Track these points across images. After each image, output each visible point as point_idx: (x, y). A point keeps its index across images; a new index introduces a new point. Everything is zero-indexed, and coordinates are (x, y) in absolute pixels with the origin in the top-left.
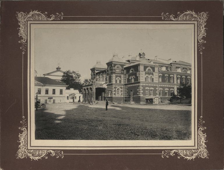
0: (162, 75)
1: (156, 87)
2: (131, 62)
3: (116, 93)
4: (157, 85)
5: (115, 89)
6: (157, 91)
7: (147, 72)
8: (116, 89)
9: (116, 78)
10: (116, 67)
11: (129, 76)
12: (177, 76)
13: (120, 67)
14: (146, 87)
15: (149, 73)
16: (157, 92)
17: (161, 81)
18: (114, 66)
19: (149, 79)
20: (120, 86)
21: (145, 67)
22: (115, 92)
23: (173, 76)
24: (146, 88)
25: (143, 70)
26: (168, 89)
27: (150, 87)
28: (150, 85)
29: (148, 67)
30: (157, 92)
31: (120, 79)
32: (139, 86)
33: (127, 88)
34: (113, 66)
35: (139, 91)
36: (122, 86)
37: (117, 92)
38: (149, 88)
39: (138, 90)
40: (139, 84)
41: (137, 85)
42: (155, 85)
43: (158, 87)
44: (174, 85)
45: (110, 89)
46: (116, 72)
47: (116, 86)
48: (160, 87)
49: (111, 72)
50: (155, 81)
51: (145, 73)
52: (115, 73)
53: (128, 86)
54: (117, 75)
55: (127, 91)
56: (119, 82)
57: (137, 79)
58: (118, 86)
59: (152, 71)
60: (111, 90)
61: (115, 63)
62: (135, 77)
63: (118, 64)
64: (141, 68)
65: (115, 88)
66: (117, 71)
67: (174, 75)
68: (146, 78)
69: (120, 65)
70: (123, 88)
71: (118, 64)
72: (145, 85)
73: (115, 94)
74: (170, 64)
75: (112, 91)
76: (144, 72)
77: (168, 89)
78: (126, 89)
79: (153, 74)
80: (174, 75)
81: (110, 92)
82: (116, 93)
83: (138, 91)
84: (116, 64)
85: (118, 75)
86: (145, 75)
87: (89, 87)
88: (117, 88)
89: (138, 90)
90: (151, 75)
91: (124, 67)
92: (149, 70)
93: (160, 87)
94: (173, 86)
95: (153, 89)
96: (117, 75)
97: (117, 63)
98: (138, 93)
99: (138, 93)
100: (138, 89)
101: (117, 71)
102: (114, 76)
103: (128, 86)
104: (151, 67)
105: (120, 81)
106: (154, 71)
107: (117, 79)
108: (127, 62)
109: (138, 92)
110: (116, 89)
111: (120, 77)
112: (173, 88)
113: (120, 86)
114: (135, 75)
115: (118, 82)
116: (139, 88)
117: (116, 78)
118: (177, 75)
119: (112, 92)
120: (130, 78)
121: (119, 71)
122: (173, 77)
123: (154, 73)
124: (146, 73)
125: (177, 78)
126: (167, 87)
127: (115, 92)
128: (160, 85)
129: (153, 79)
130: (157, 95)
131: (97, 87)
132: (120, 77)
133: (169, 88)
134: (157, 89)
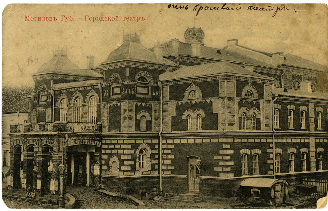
0: (279, 107)
1: (264, 146)
4: (269, 140)
6: (270, 159)
7: (244, 101)
8: (138, 151)
9: (136, 116)
11: (180, 109)
12: (315, 110)
13: (150, 80)
14: (241, 149)
15: (249, 101)
16: (269, 162)
17: (278, 127)
19: (249, 121)
20: (149, 141)
23: (305, 108)
24: (243, 151)
25: (234, 95)
26: (295, 150)
27: (251, 149)
28: (251, 141)
29: (247, 83)
30: (269, 162)
31: (148, 118)
33: (172, 147)
36: (154, 141)
37: (137, 160)
38: (248, 151)
39: (217, 157)
41: (214, 141)
42: (263, 140)
43: (271, 145)
44: (309, 136)
45: (114, 152)
47: (138, 142)
48: (277, 145)
50: (264, 129)
53: (177, 141)
54: (139, 104)
58: (141, 141)
59: (256, 96)
62: (203, 115)
63: (143, 70)
67: (307, 106)
68: (240, 119)
70: (156, 146)
71: (143, 70)
72: (239, 140)
76: (236, 102)
77: (295, 150)
78: (169, 151)
79: (258, 106)
80: (307, 106)
81: (115, 158)
82: (137, 164)
84: (139, 70)
85: (143, 104)
89: (217, 157)
90: (253, 110)
92: (249, 94)
93: (277, 145)
94: (307, 140)
95: (259, 151)
96: (139, 104)
98: (216, 169)
99: (216, 169)
100: (220, 155)
101: (139, 90)
103: (177, 141)
104: (254, 84)
106: (261, 96)
107: (138, 118)
109: (218, 166)
110: (138, 151)
112: (307, 145)
113: (149, 141)
114: (207, 108)
115: (143, 125)
117: (136, 116)
118: (315, 106)
120: (184, 117)
122: (307, 113)
123: (262, 103)
124: (240, 105)
125: (316, 114)
126: (293, 145)
129: (258, 120)
130: (269, 172)
134: (269, 151)
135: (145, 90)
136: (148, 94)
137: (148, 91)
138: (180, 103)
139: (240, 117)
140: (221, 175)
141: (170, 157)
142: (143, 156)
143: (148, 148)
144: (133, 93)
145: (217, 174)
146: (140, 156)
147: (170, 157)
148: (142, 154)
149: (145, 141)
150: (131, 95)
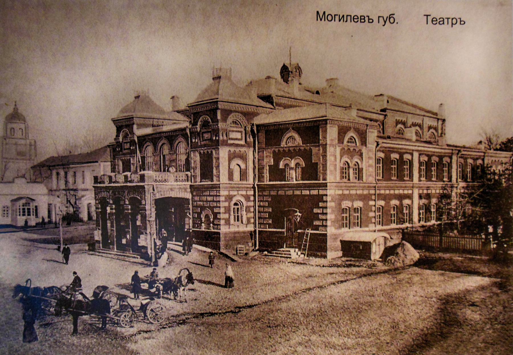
0: (382, 155)
2: (277, 104)
3: (232, 217)
5: (226, 204)
7: (346, 148)
10: (231, 119)
15: (352, 149)
18: (225, 120)
21: (342, 132)
22: (226, 216)
23: (408, 157)
29: (348, 129)
32: (320, 198)
34: (219, 117)
35: (321, 217)
37: (232, 213)
39: (315, 211)
40: (321, 192)
41: (314, 192)
42: (366, 192)
43: (373, 197)
46: (230, 142)
47: (232, 193)
49: (211, 140)
51: (341, 150)
52: (225, 143)
53: (273, 193)
55: (270, 210)
56: (237, 175)
57: (312, 171)
58: (235, 193)
60: (212, 208)
61: (227, 106)
64: (332, 133)
65: (229, 198)
66: (233, 135)
69: (242, 113)
73: (227, 222)
74: (382, 111)
75: (216, 210)
76: (338, 150)
80: (412, 155)
82: (232, 217)
83: (318, 214)
86: (341, 157)
87: (238, 252)
88: (234, 201)
89: (315, 211)
90: (356, 159)
91: (257, 121)
92: (351, 140)
97: (233, 107)
98: (316, 223)
99: (316, 223)
100: (319, 207)
101: (233, 135)
102: (223, 153)
105: (243, 175)
106: (364, 142)
108: (261, 101)
109: (319, 219)
111: (243, 157)
113: (244, 193)
114: (307, 155)
116: (321, 204)
117: (229, 164)
118: (420, 155)
119: (215, 215)
120: (281, 166)
121: (240, 137)
122: (411, 162)
123: (364, 150)
125: (420, 164)
127: (226, 216)
128: (378, 192)
130: (370, 225)
131: (158, 196)
132: (243, 157)
133: (401, 198)
135: (238, 135)
136: (241, 139)
137: (242, 137)
138: (277, 150)
139: (342, 166)
140: (320, 228)
141: (266, 210)
142: (238, 209)
143: (243, 200)
144: (225, 138)
145: (316, 228)
146: (234, 208)
147: (266, 210)
148: (236, 207)
149: (240, 192)
150: (223, 141)
